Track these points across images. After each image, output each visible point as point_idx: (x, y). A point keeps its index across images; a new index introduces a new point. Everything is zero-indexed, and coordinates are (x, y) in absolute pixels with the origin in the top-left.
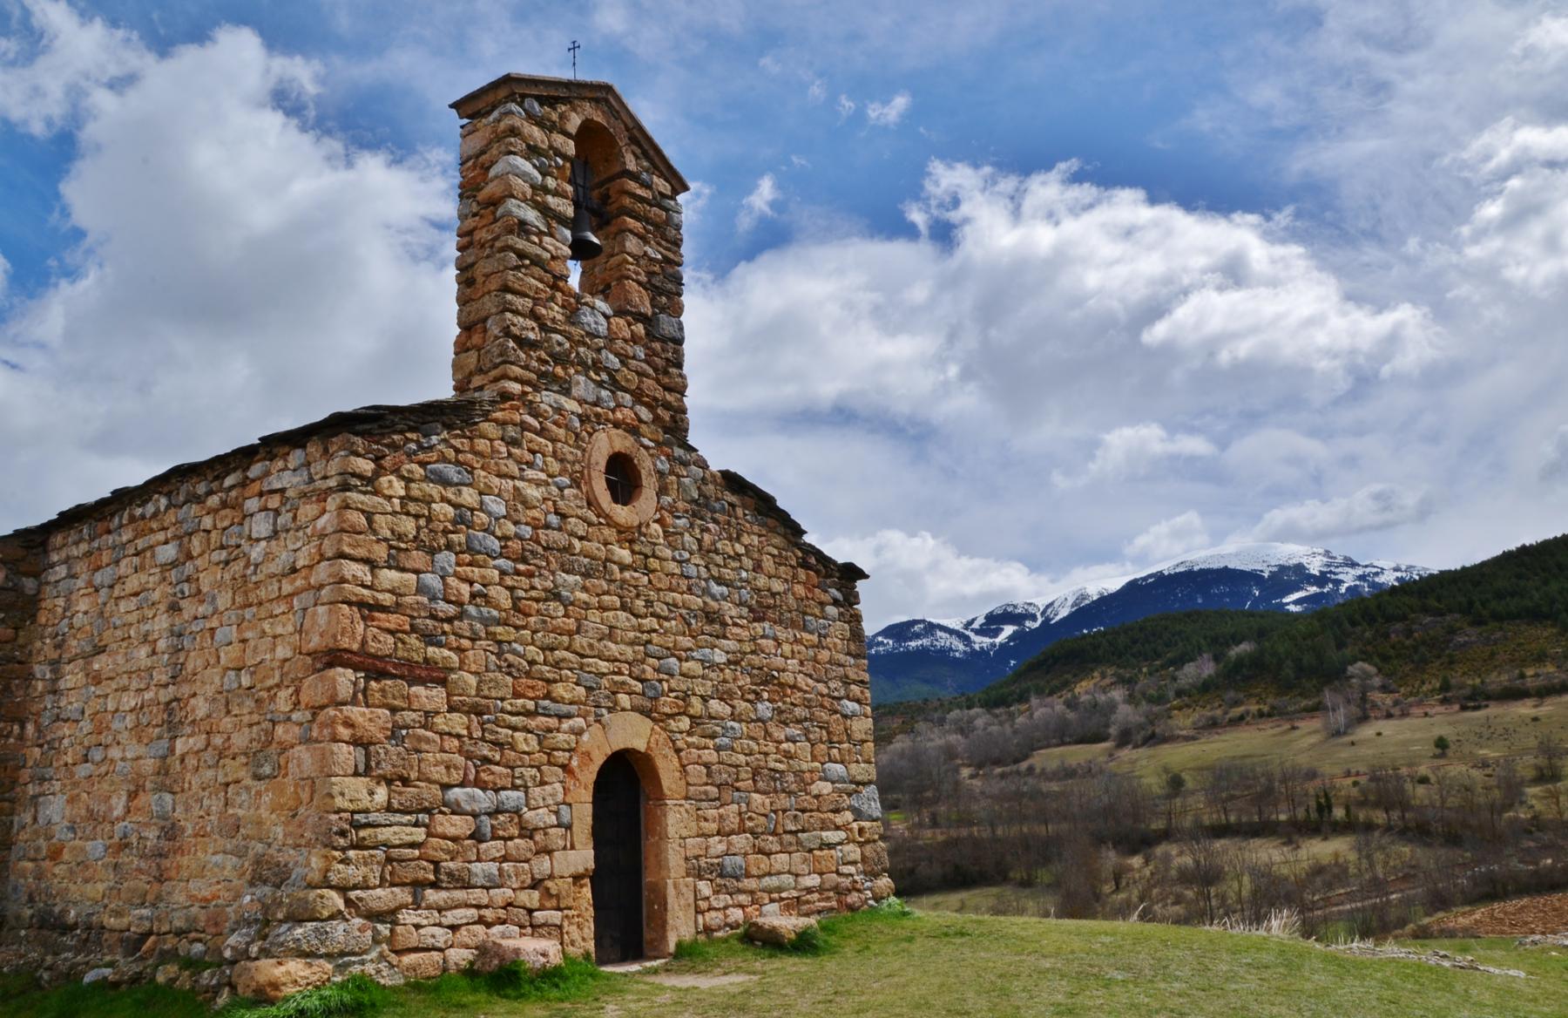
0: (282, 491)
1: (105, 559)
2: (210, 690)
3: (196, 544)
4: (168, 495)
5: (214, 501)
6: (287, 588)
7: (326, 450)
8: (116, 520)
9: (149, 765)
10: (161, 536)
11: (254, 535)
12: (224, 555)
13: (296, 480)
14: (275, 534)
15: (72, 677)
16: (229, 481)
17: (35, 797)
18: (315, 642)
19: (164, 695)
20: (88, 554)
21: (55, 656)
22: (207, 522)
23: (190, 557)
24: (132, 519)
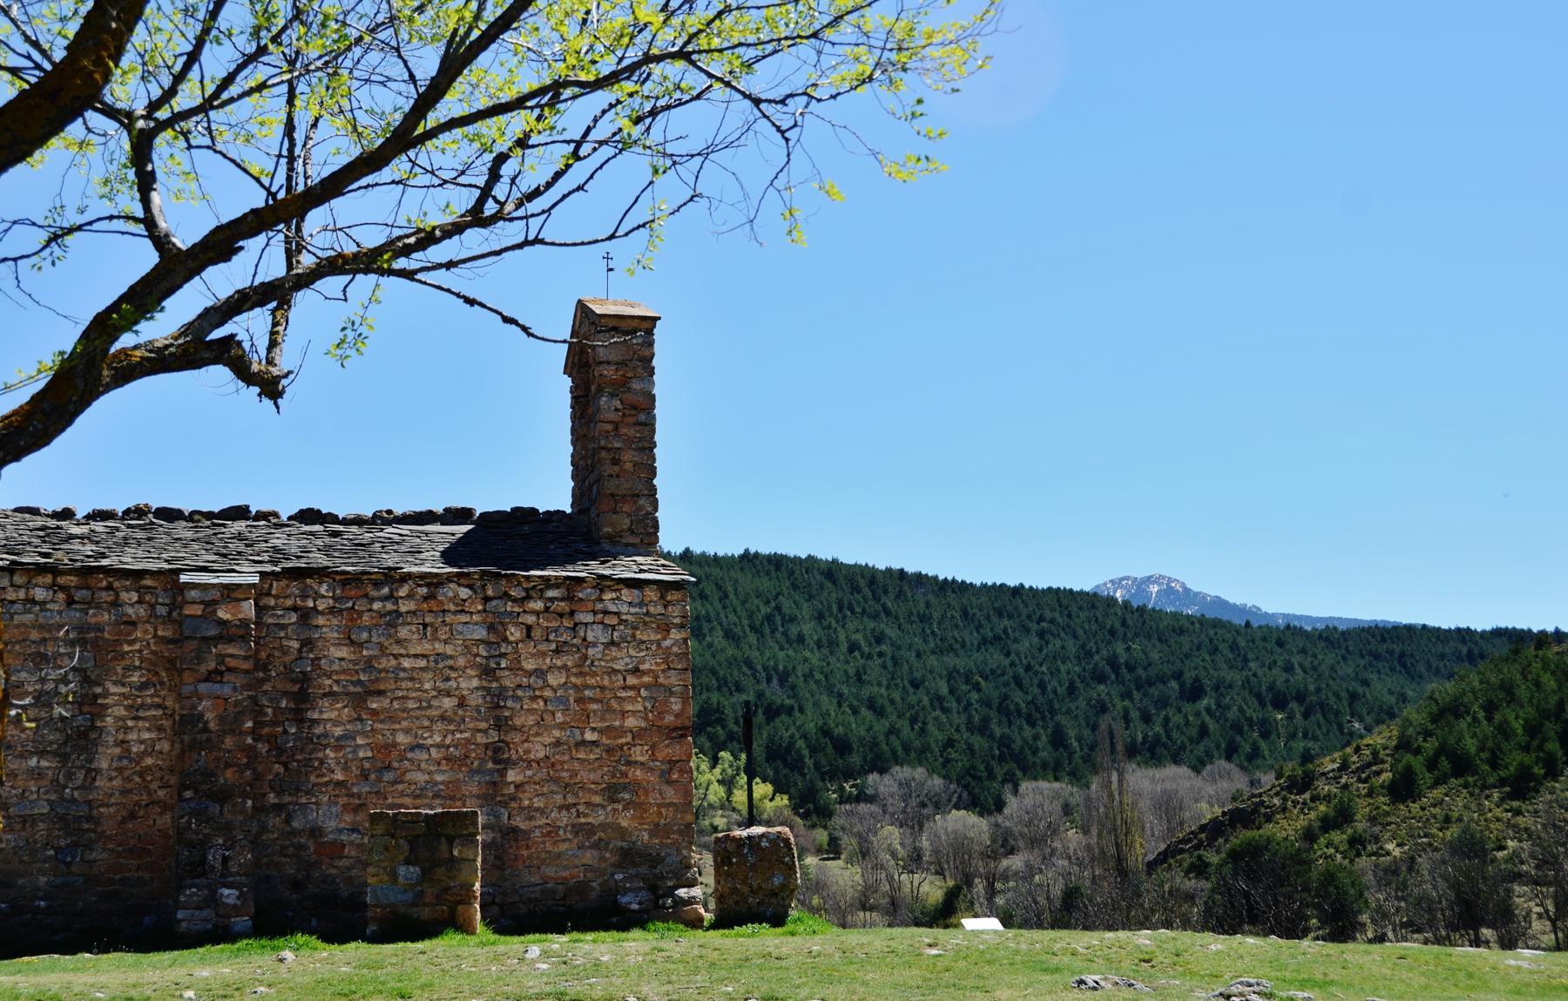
0: (617, 614)
1: (366, 617)
2: (548, 740)
3: (515, 633)
4: (470, 587)
5: (538, 605)
6: (632, 680)
7: (662, 597)
8: (386, 590)
9: (472, 788)
10: (464, 618)
11: (590, 638)
12: (553, 646)
13: (633, 610)
14: (613, 643)
15: (331, 716)
16: (550, 594)
17: (278, 808)
18: (669, 719)
19: (480, 738)
20: (331, 611)
21: (296, 688)
22: (530, 619)
23: (505, 639)
24: (410, 596)
